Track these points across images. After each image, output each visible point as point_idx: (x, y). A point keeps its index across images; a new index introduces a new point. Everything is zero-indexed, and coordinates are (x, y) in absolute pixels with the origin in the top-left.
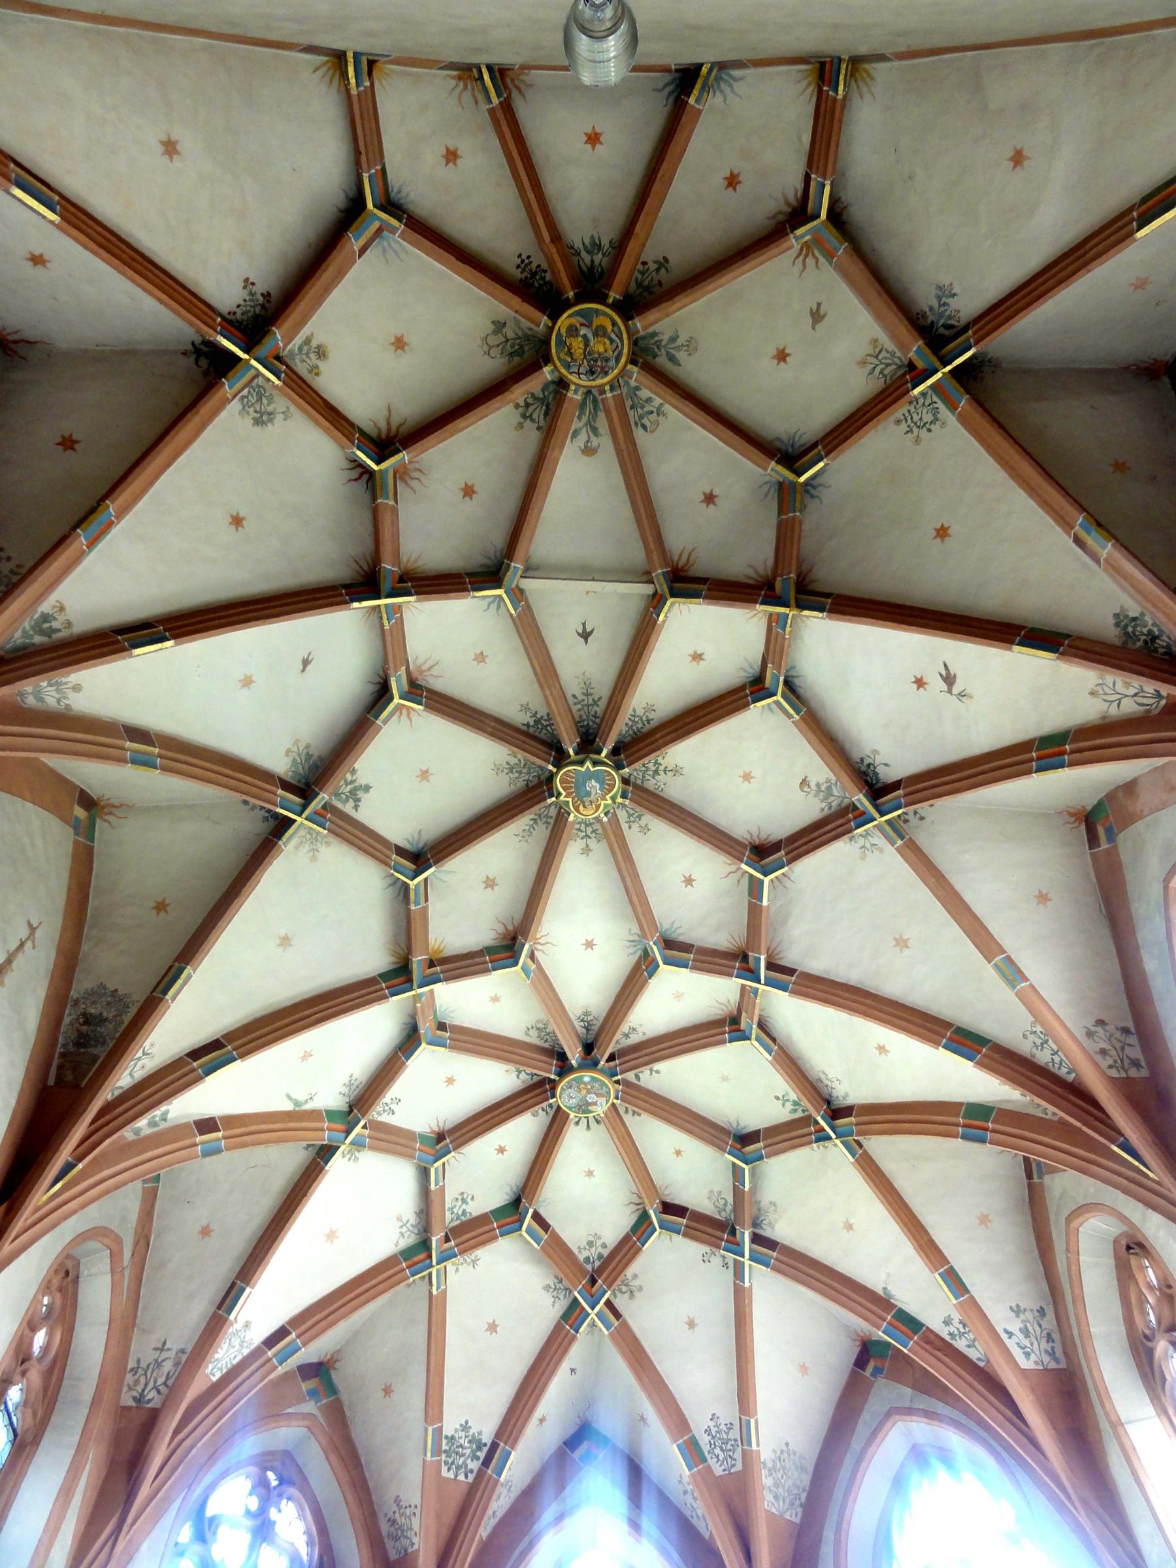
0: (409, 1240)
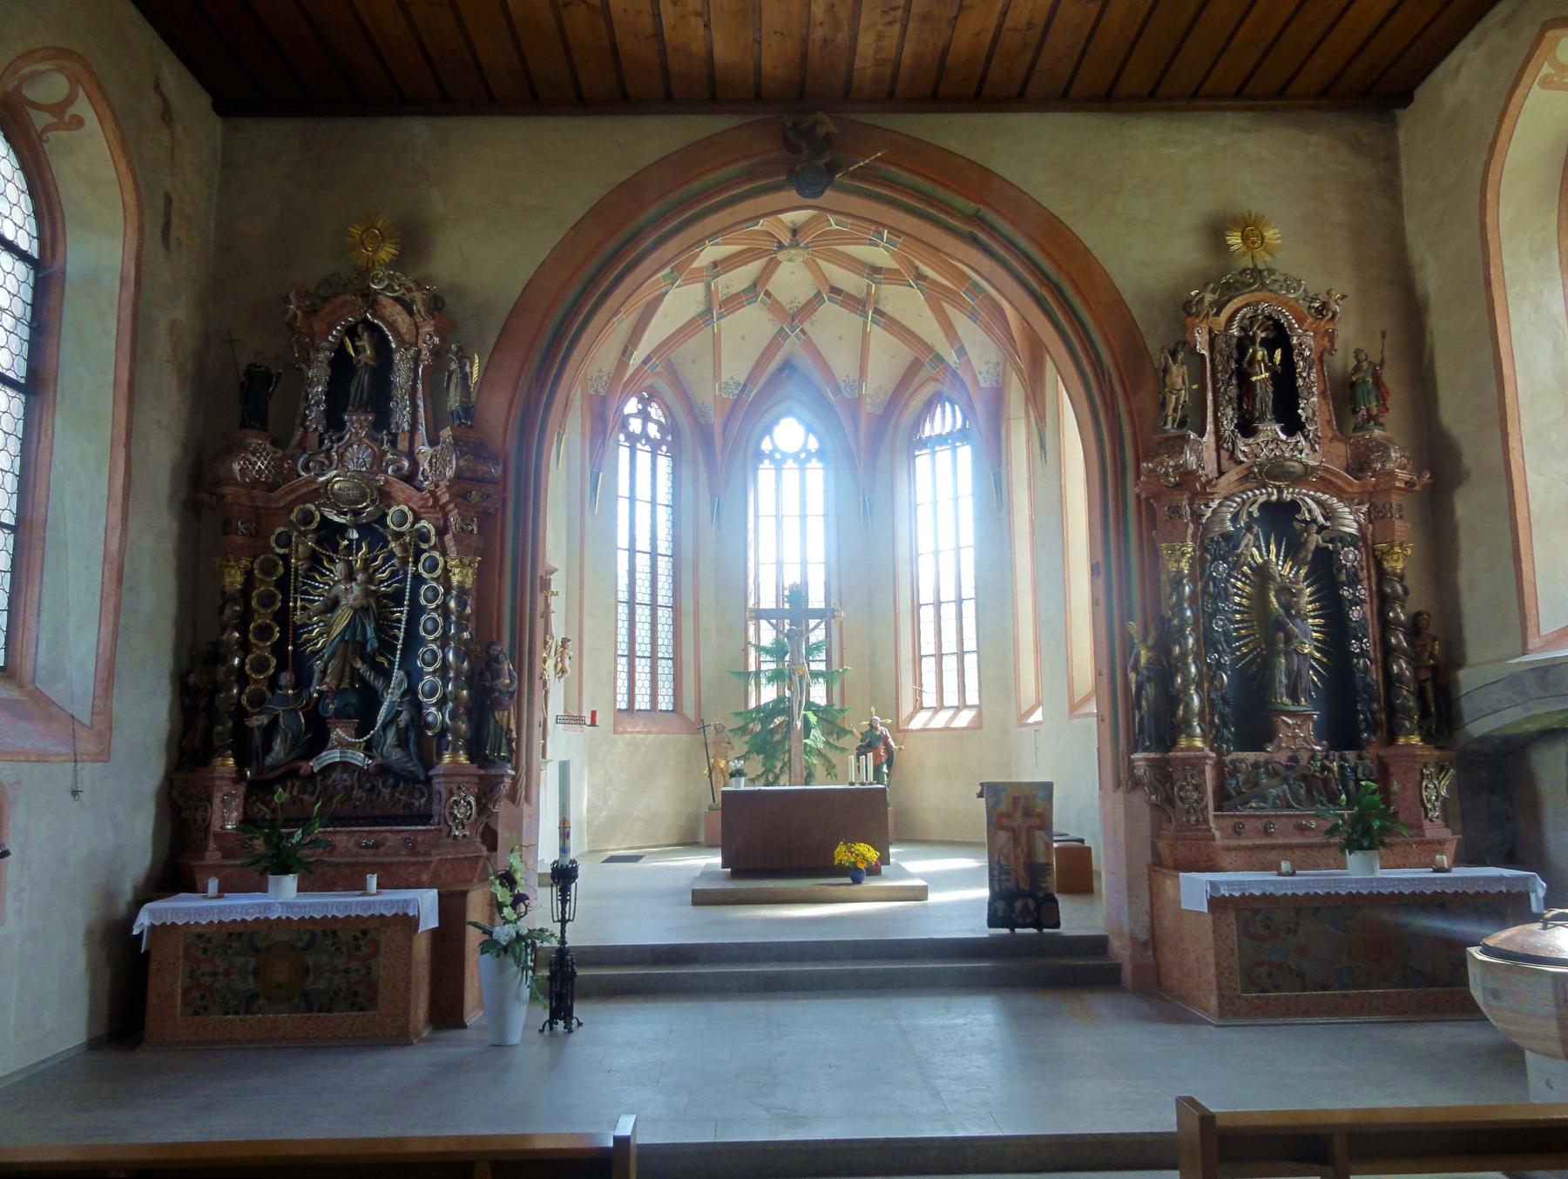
0: (702, 308)
